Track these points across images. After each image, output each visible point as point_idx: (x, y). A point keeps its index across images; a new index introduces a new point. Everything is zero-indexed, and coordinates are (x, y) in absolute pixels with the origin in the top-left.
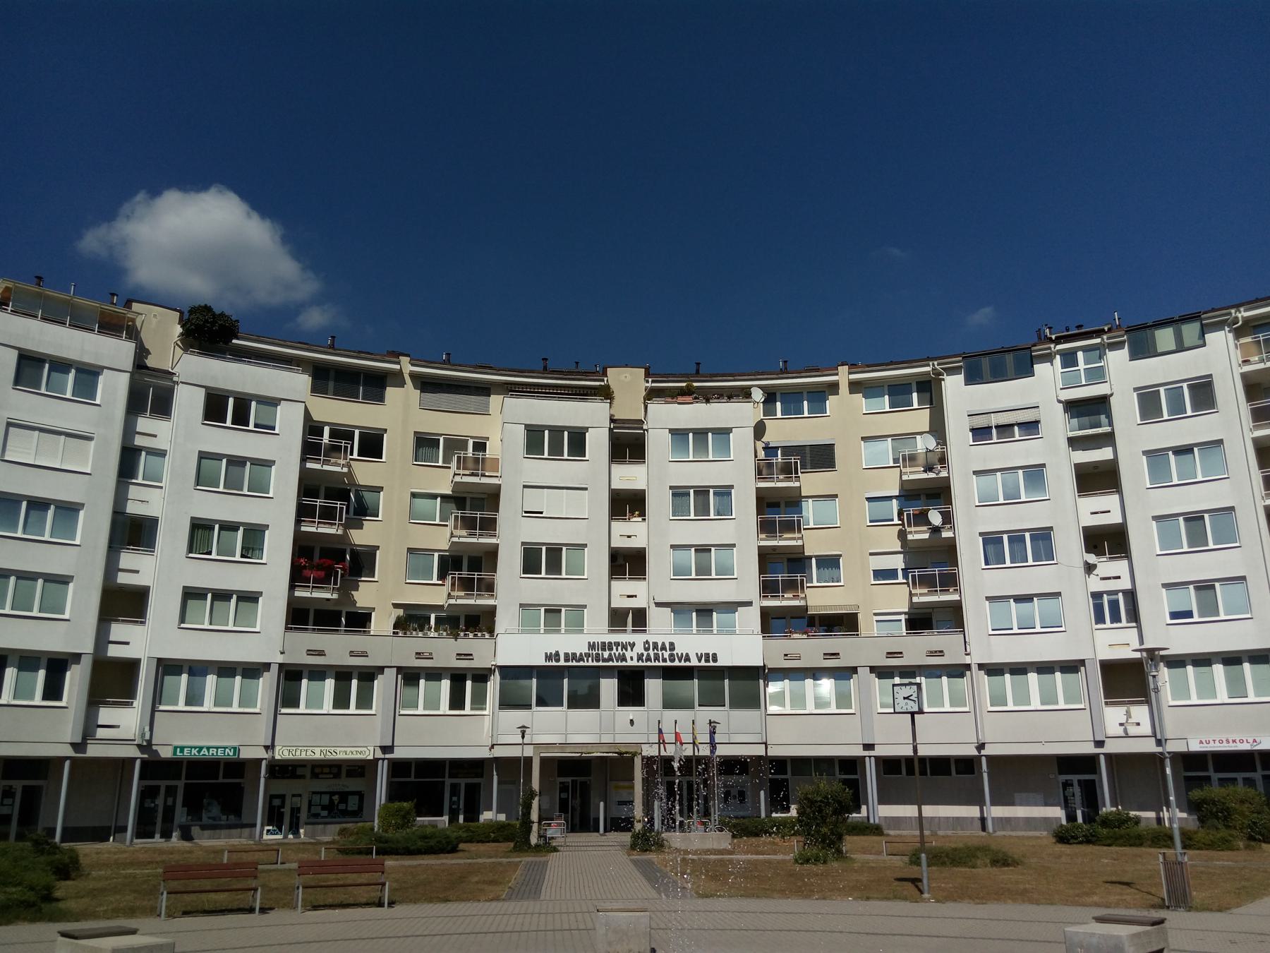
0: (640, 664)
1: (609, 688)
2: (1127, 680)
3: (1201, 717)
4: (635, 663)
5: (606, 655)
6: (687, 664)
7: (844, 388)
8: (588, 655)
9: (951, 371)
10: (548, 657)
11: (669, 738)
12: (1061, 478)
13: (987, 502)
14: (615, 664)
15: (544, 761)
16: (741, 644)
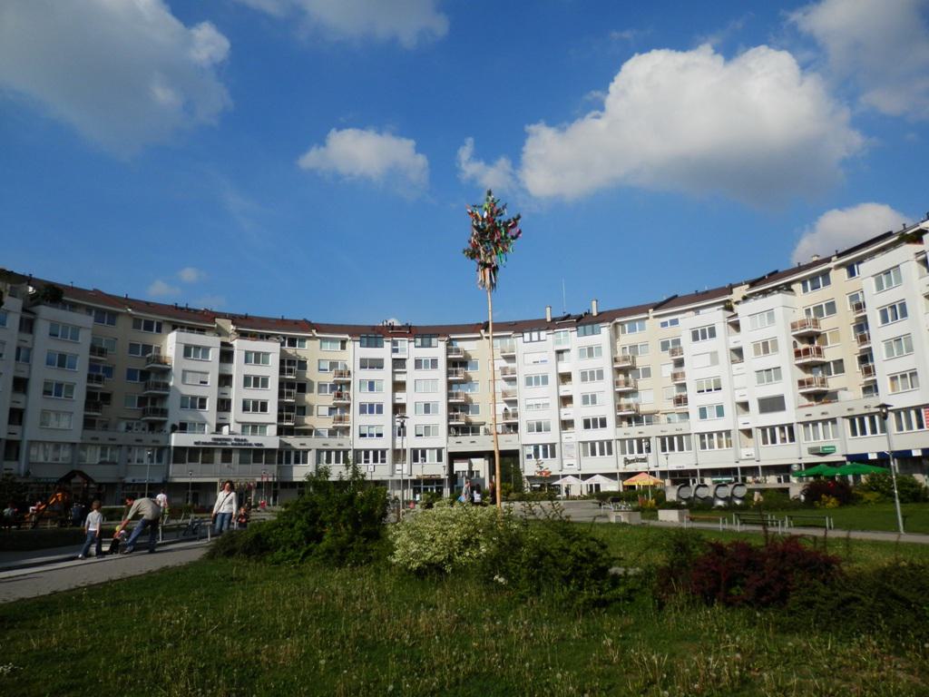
1: (218, 456)
10: (196, 443)
16: (270, 439)
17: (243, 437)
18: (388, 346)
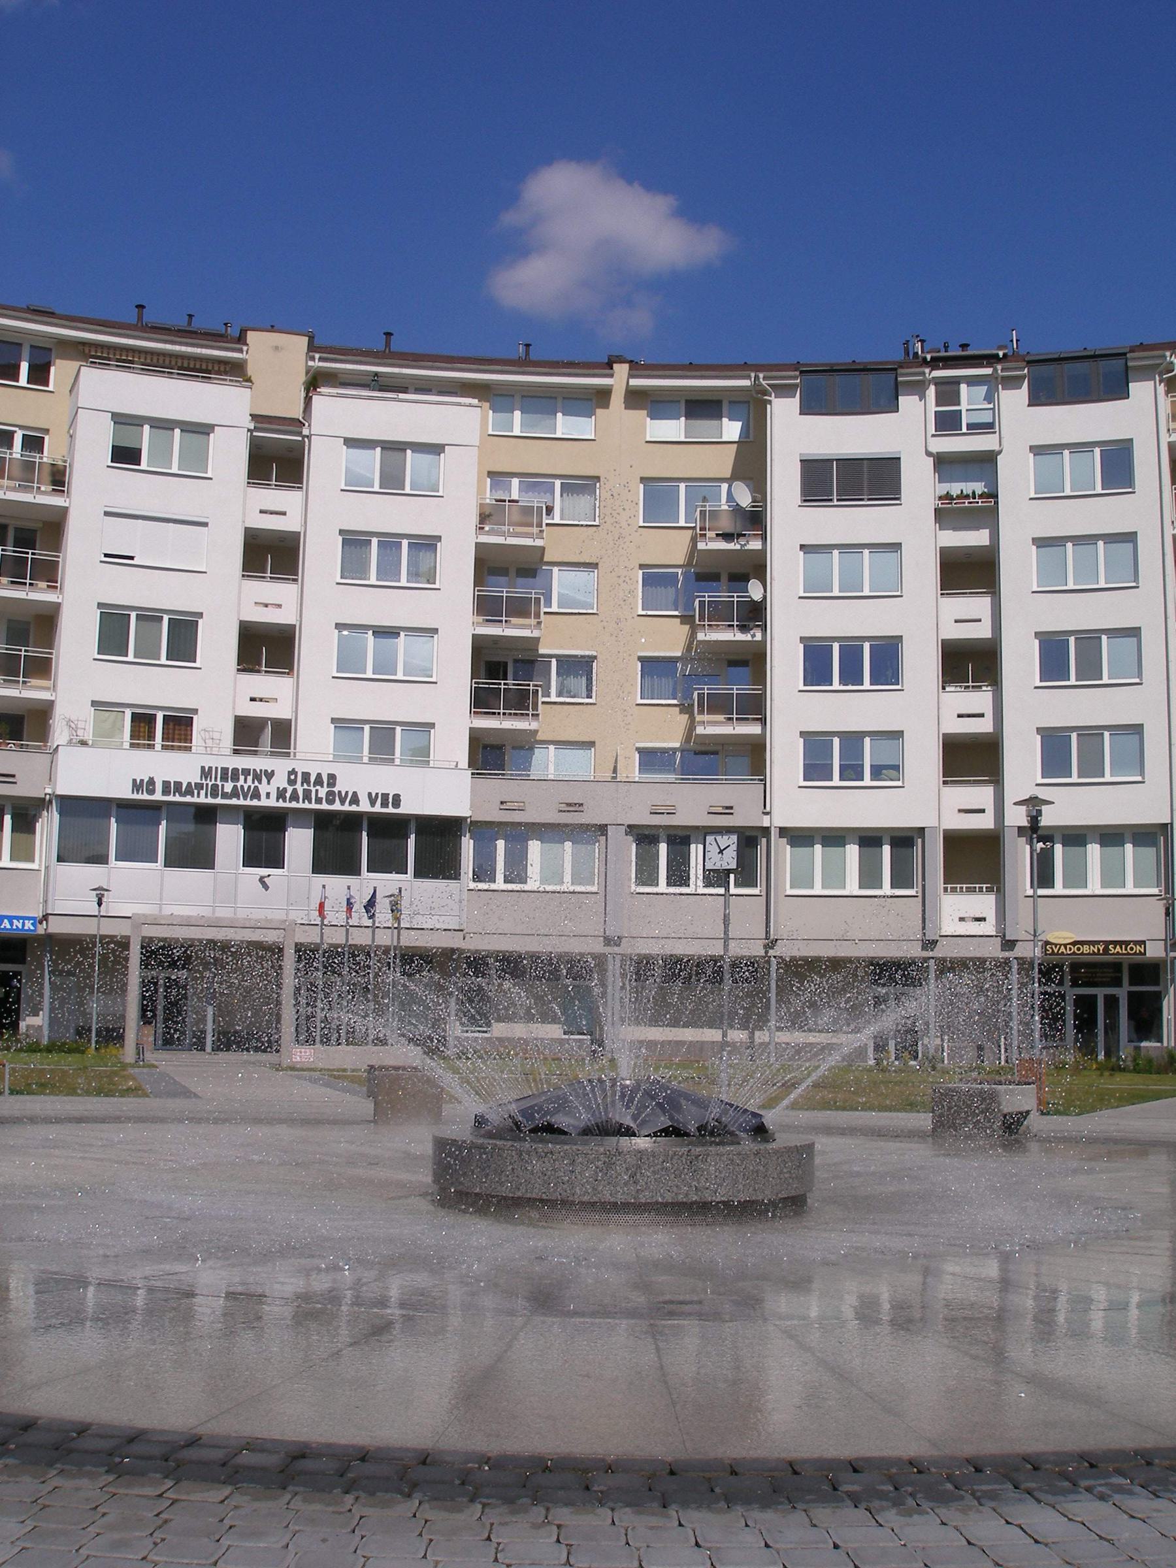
0: (281, 804)
1: (229, 838)
2: (974, 858)
3: (1100, 904)
4: (272, 802)
5: (228, 787)
6: (354, 808)
7: (617, 399)
8: (199, 786)
9: (784, 391)
10: (137, 786)
12: (922, 569)
13: (816, 590)
14: (241, 802)
15: (146, 944)
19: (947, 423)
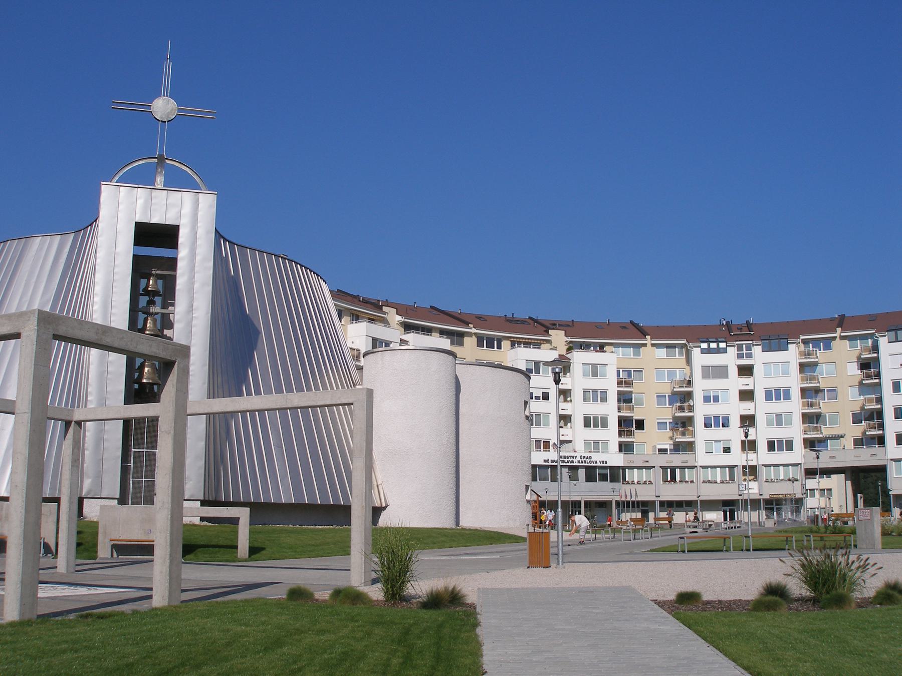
4: (577, 464)
7: (649, 345)
10: (545, 461)
11: (628, 494)
15: (586, 502)
17: (589, 455)
18: (732, 351)
19: (740, 356)
